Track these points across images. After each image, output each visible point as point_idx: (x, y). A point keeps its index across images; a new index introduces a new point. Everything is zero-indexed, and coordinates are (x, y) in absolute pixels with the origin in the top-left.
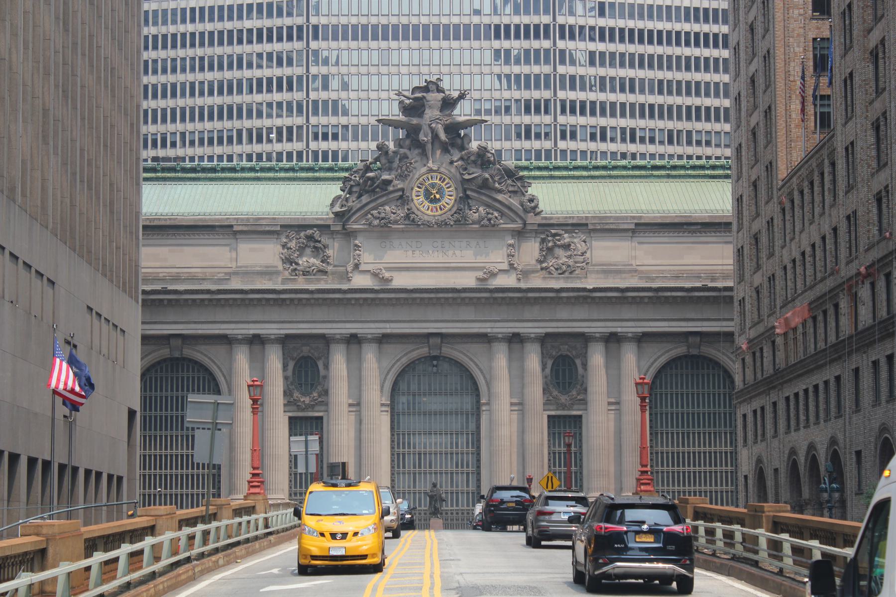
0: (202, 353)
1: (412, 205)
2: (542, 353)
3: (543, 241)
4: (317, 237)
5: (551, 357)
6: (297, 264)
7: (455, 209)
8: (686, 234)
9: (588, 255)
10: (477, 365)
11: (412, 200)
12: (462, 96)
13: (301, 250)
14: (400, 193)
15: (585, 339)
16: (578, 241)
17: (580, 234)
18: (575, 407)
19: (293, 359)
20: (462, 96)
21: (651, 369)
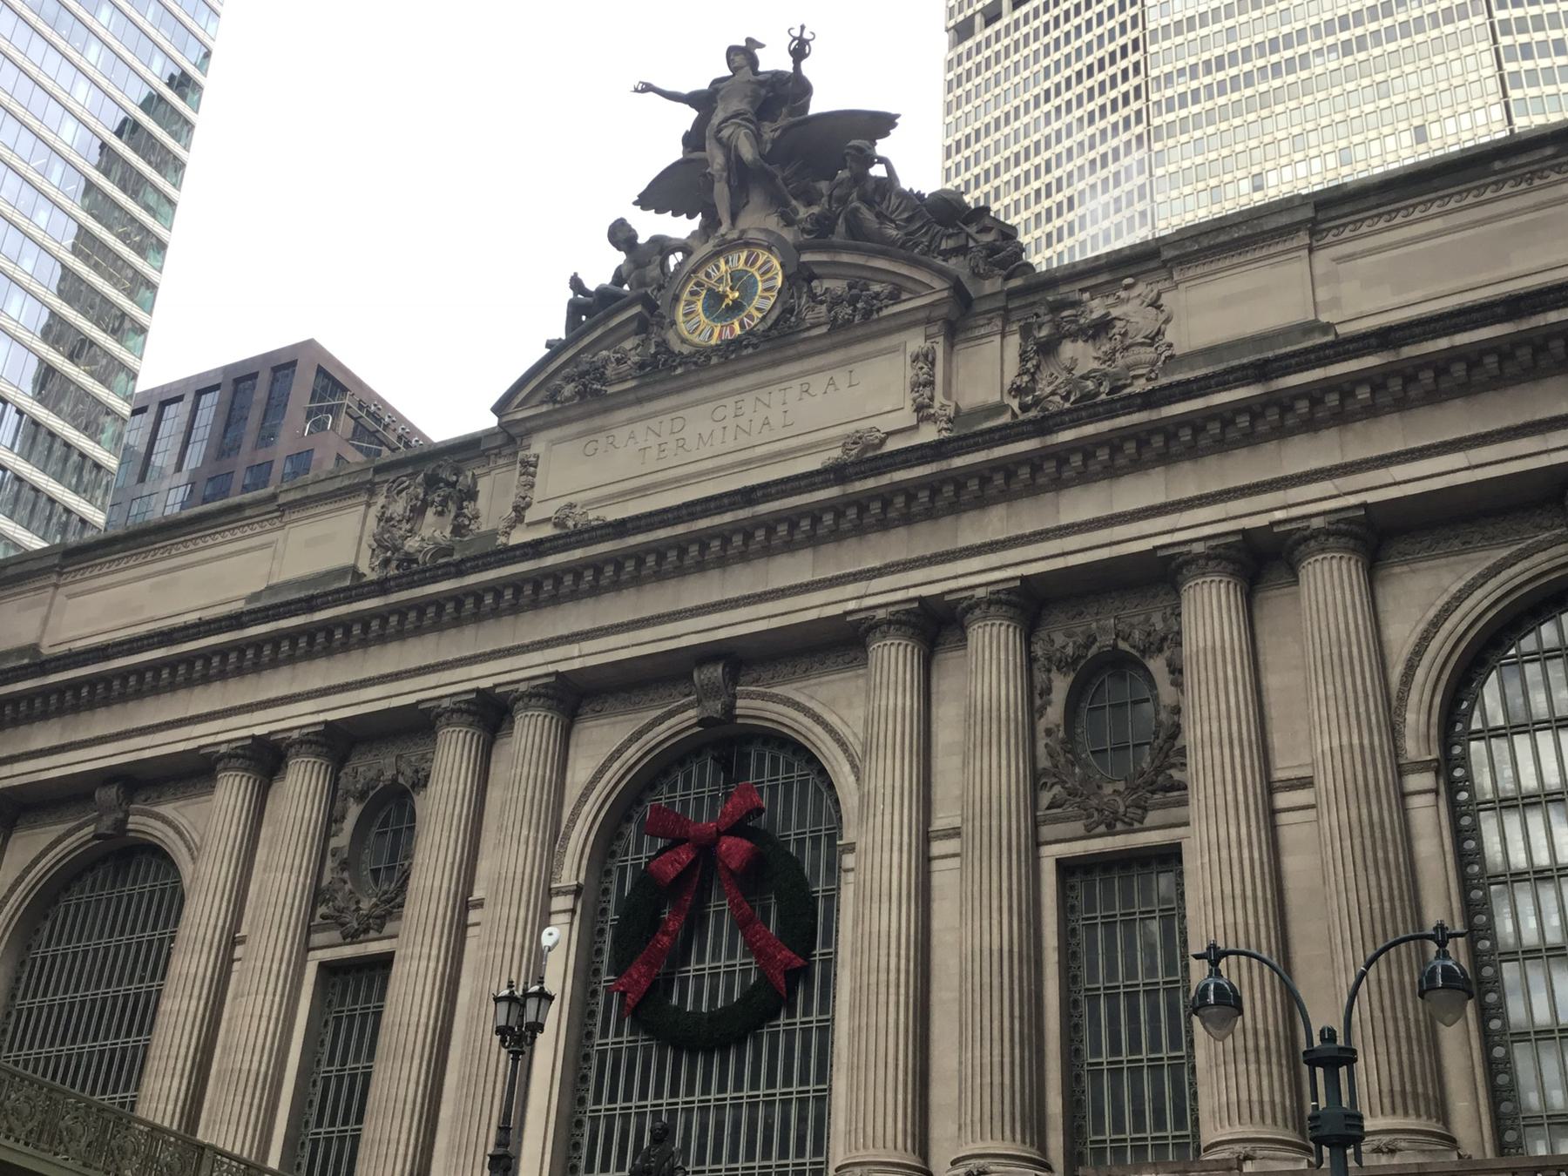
0: (164, 820)
1: (670, 335)
2: (1031, 660)
3: (1026, 332)
4: (446, 474)
5: (1064, 665)
6: (396, 549)
7: (774, 315)
8: (1506, 190)
9: (1169, 336)
10: (831, 730)
11: (673, 323)
12: (799, 51)
13: (418, 512)
14: (637, 309)
15: (1160, 575)
16: (1130, 308)
17: (1141, 288)
18: (1153, 817)
19: (361, 796)
20: (799, 51)
21: (1434, 645)
